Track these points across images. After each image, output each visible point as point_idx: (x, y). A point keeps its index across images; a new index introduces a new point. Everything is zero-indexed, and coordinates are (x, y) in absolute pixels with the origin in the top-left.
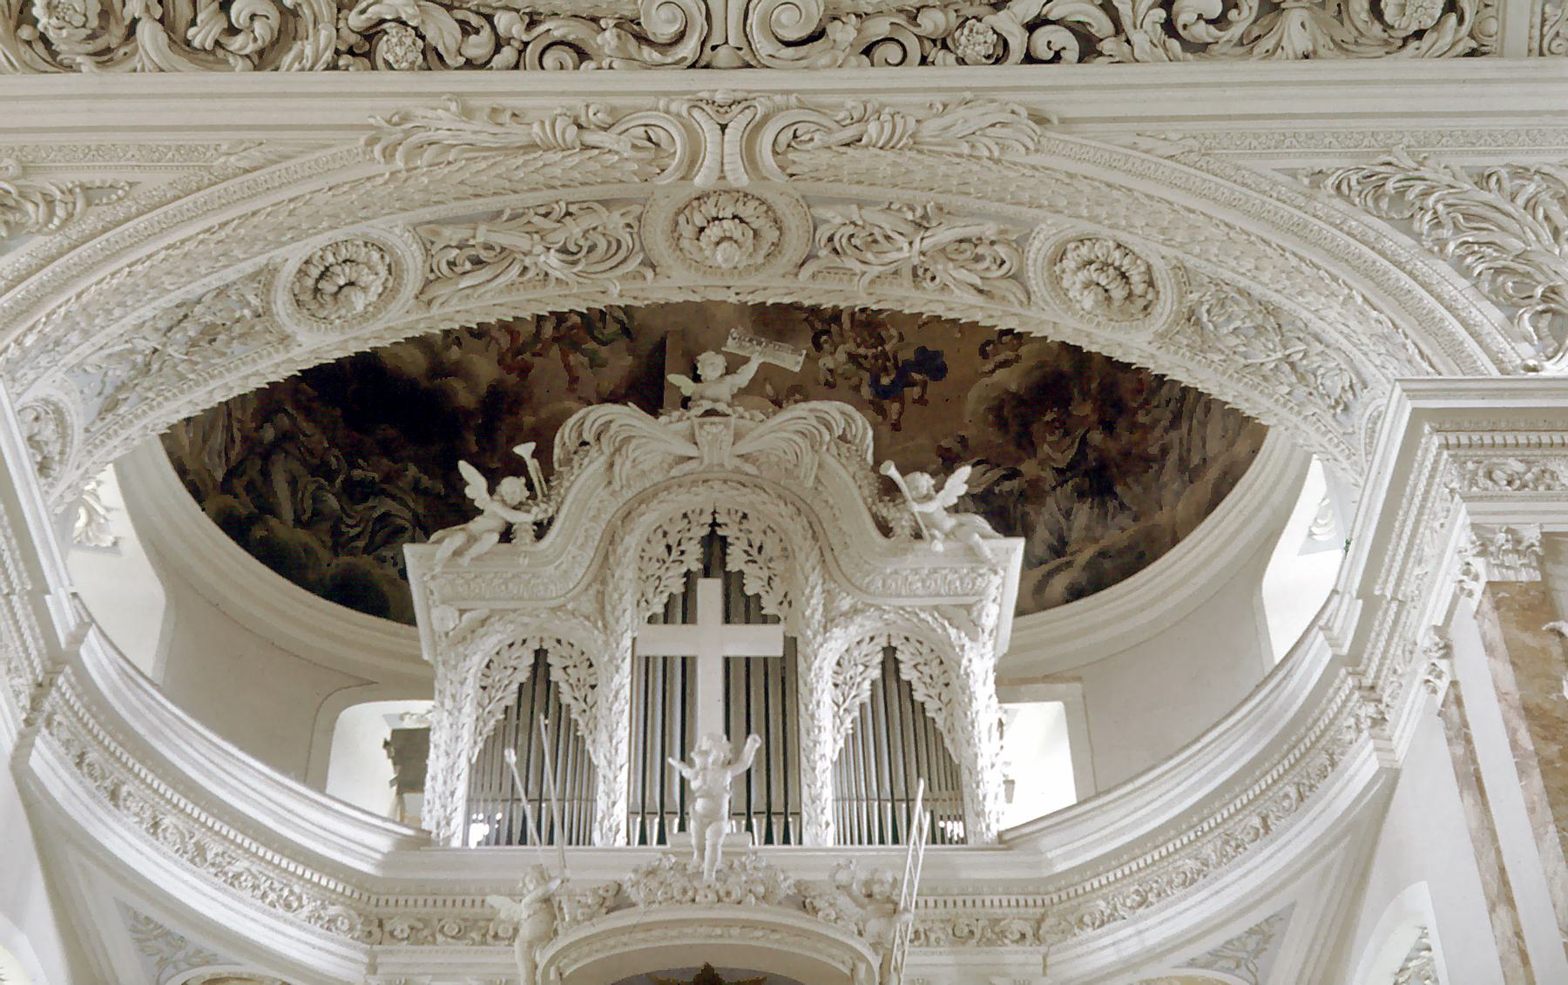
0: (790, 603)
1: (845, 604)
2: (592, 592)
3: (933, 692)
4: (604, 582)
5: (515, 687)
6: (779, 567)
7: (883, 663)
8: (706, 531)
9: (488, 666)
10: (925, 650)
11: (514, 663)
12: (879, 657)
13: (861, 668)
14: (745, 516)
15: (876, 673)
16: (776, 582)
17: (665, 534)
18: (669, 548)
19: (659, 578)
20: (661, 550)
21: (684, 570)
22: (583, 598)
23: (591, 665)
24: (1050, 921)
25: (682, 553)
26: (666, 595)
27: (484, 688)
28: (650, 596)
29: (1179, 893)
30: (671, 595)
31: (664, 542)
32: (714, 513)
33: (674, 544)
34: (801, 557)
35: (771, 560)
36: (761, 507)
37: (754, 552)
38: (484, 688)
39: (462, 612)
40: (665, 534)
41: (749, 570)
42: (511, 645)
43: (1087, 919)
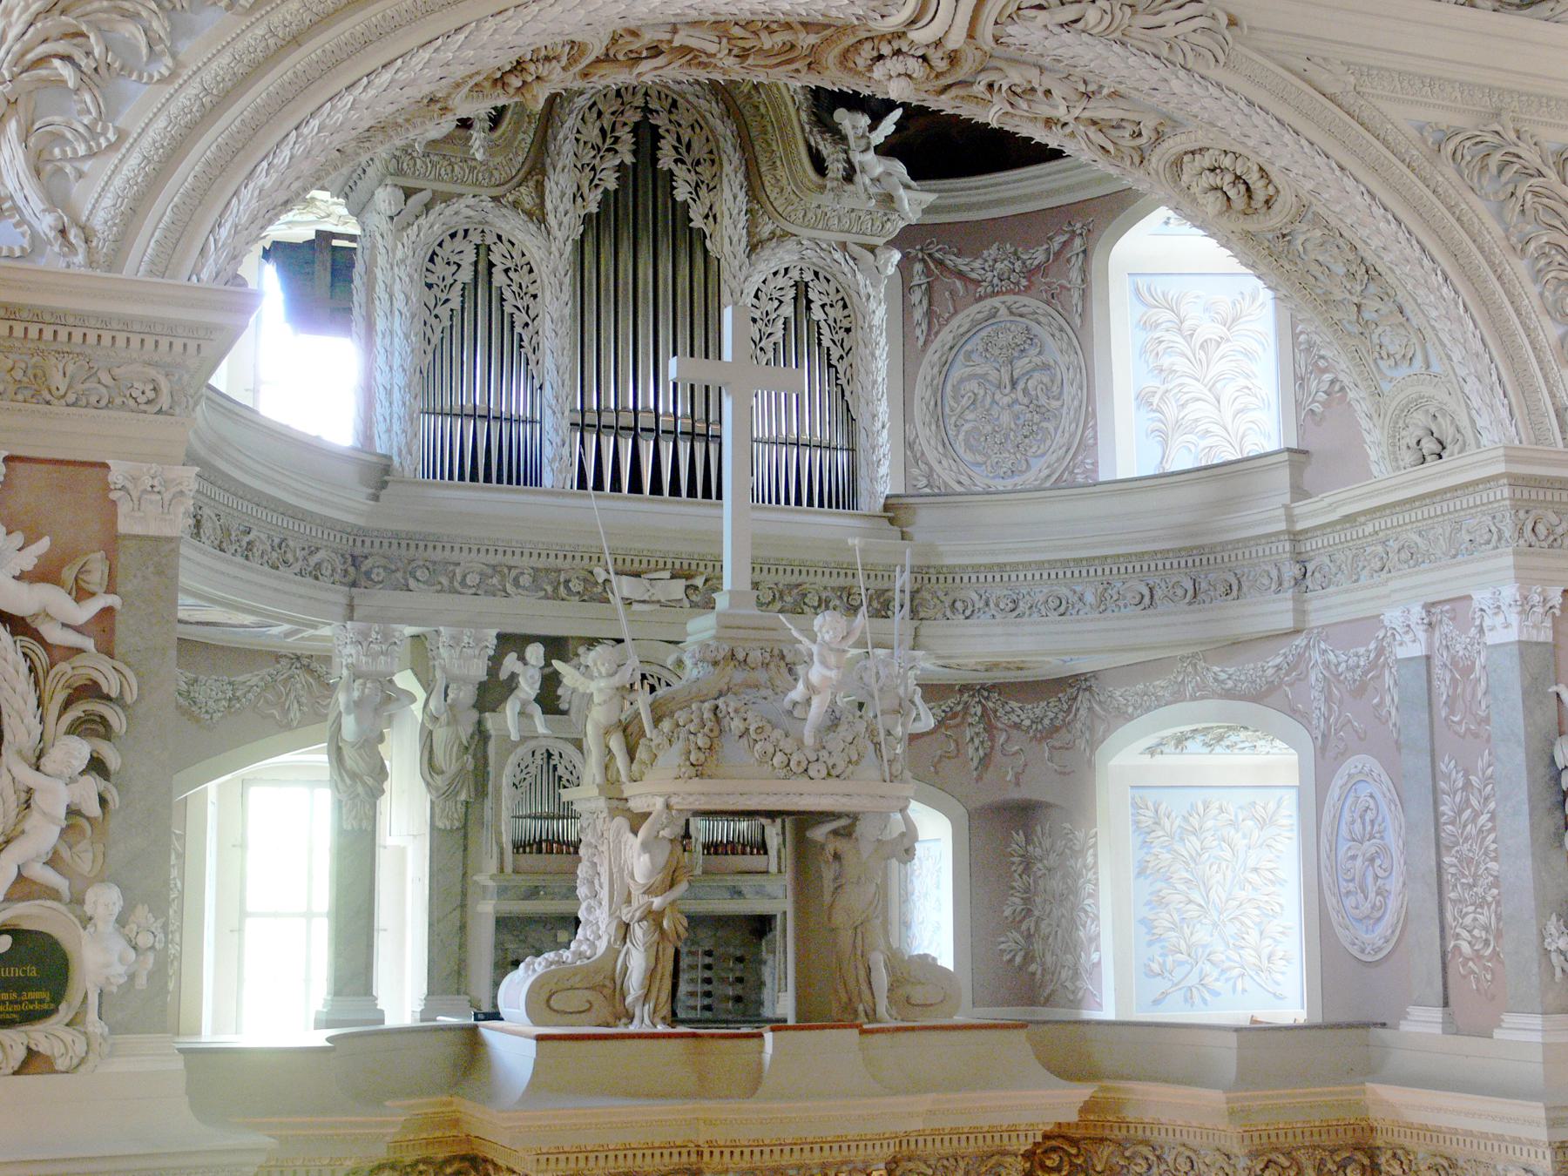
0: (715, 217)
1: (765, 230)
2: (531, 184)
3: (836, 338)
4: (544, 173)
5: (459, 286)
6: (706, 171)
7: (795, 299)
8: (637, 117)
9: (431, 260)
10: (832, 291)
11: (456, 258)
12: (792, 293)
13: (776, 303)
14: (674, 104)
15: (788, 310)
16: (703, 191)
17: (600, 114)
18: (602, 130)
19: (593, 169)
20: (592, 134)
21: (617, 162)
22: (522, 189)
23: (531, 271)
24: (925, 595)
25: (617, 139)
26: (601, 189)
27: (430, 286)
28: (585, 190)
29: (1054, 616)
30: (606, 191)
31: (598, 124)
32: (646, 94)
33: (608, 127)
34: (727, 168)
35: (698, 163)
36: (691, 98)
37: (683, 150)
38: (430, 286)
39: (409, 193)
40: (600, 114)
41: (676, 170)
42: (453, 236)
43: (959, 605)
